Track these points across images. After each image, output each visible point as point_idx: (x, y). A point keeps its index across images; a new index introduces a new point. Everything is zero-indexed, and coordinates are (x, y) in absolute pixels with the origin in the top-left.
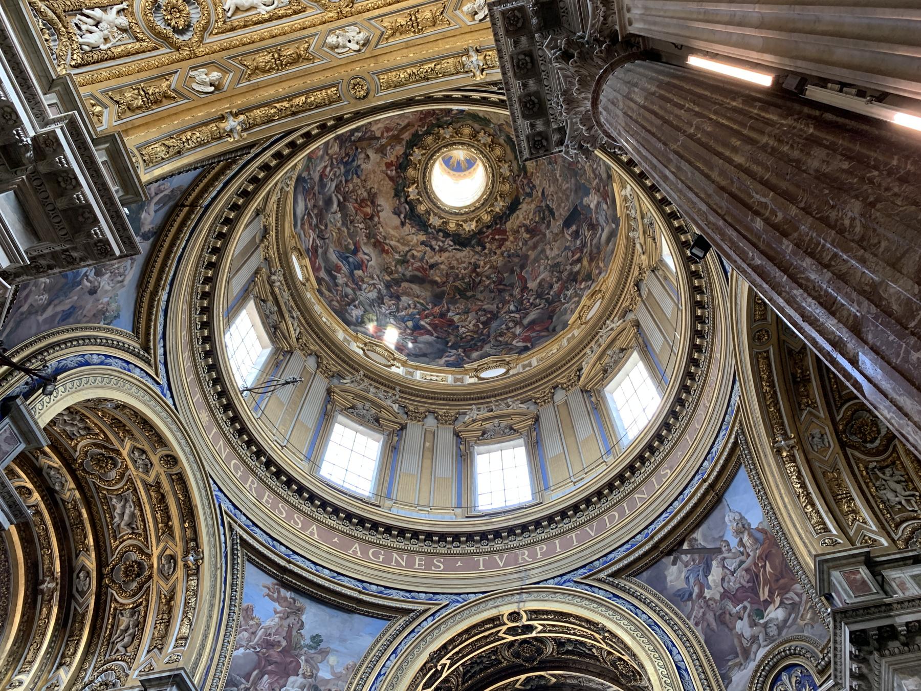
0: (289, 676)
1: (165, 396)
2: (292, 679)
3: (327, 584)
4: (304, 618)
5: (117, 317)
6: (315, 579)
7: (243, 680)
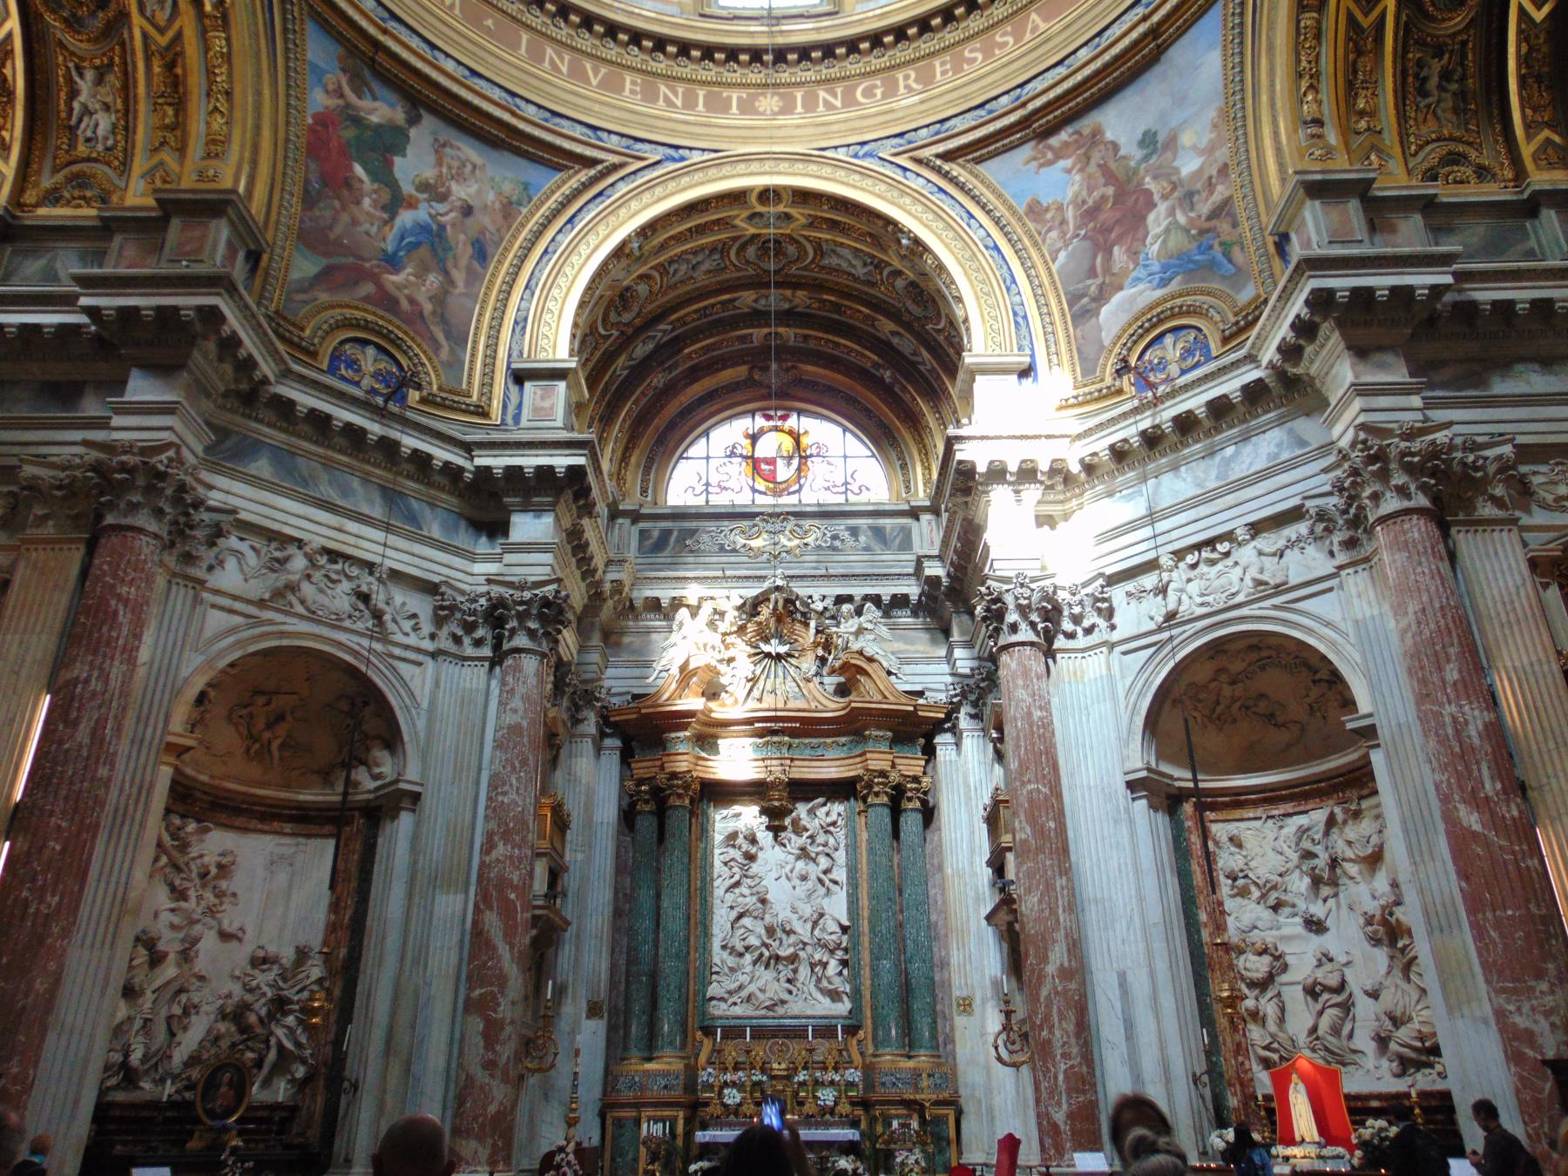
0: (1144, 218)
1: (683, 159)
2: (1151, 217)
3: (1098, 64)
4: (1109, 136)
5: (526, 186)
6: (1079, 77)
7: (1089, 282)
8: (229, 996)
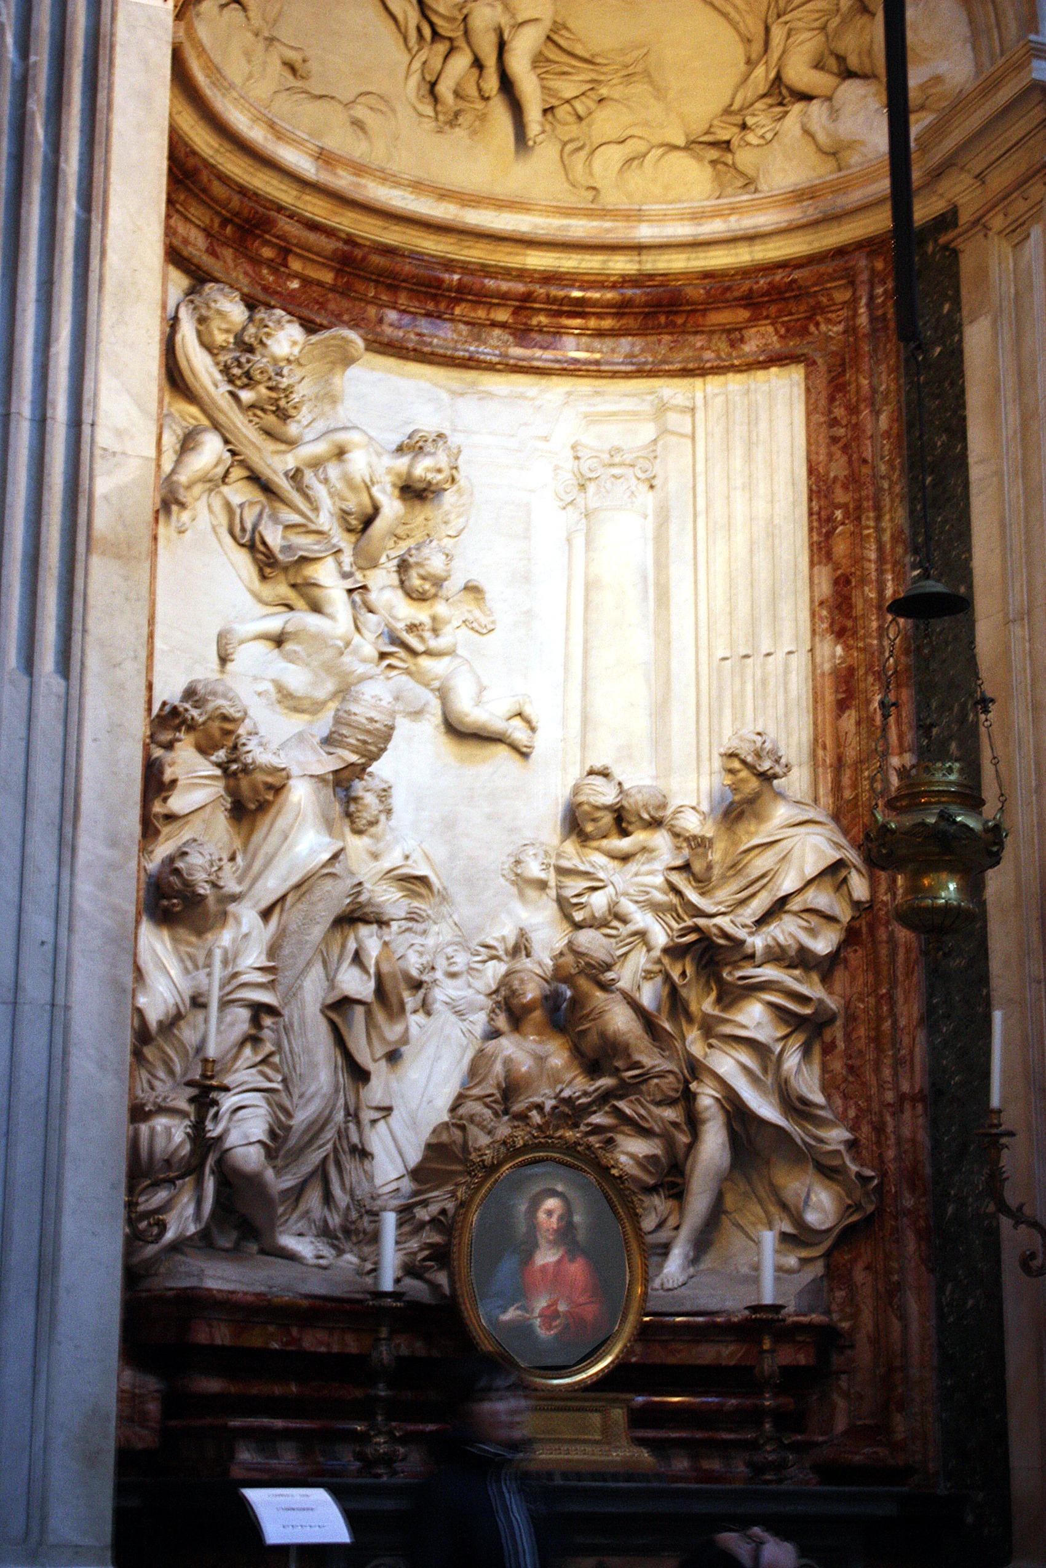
8: (520, 948)
